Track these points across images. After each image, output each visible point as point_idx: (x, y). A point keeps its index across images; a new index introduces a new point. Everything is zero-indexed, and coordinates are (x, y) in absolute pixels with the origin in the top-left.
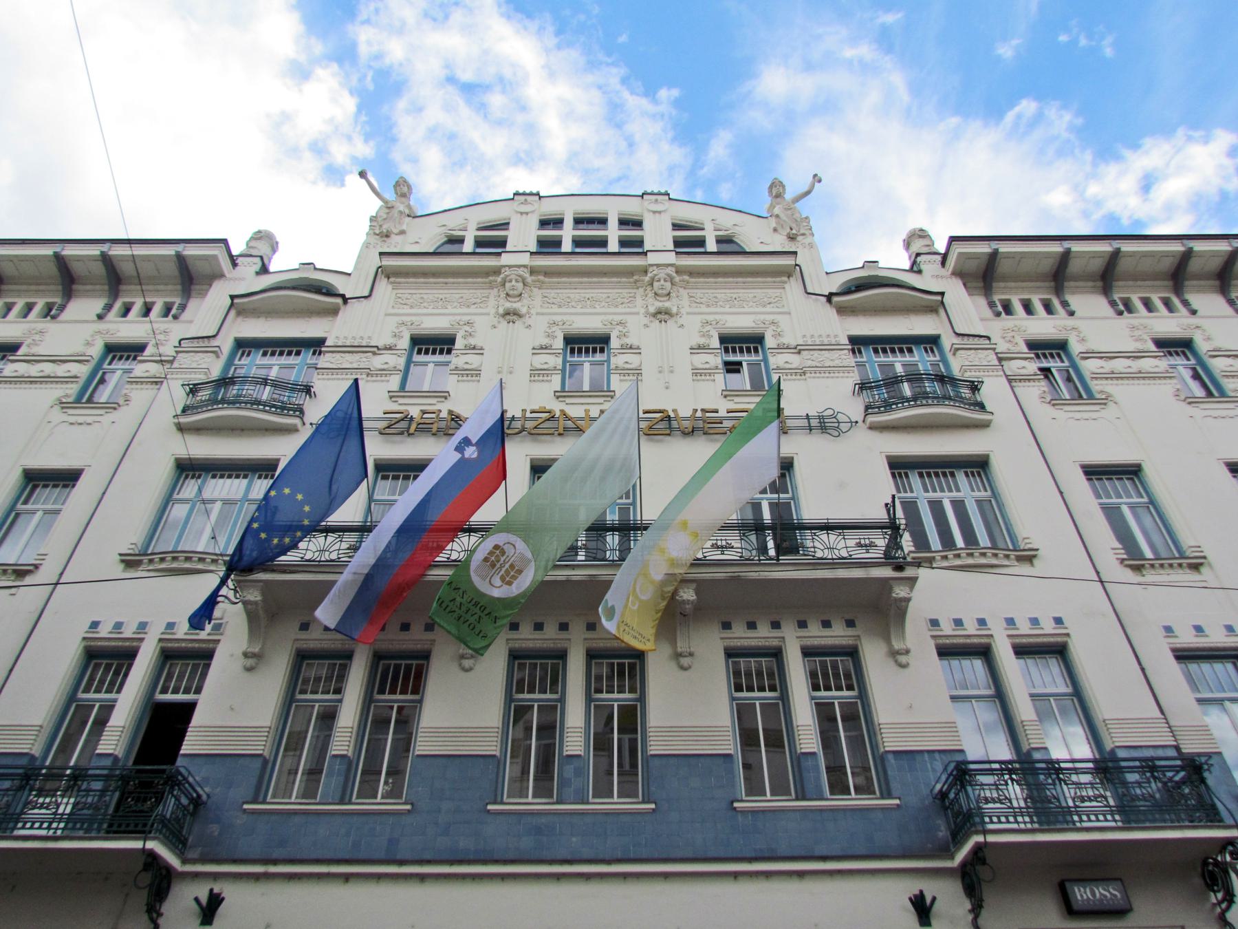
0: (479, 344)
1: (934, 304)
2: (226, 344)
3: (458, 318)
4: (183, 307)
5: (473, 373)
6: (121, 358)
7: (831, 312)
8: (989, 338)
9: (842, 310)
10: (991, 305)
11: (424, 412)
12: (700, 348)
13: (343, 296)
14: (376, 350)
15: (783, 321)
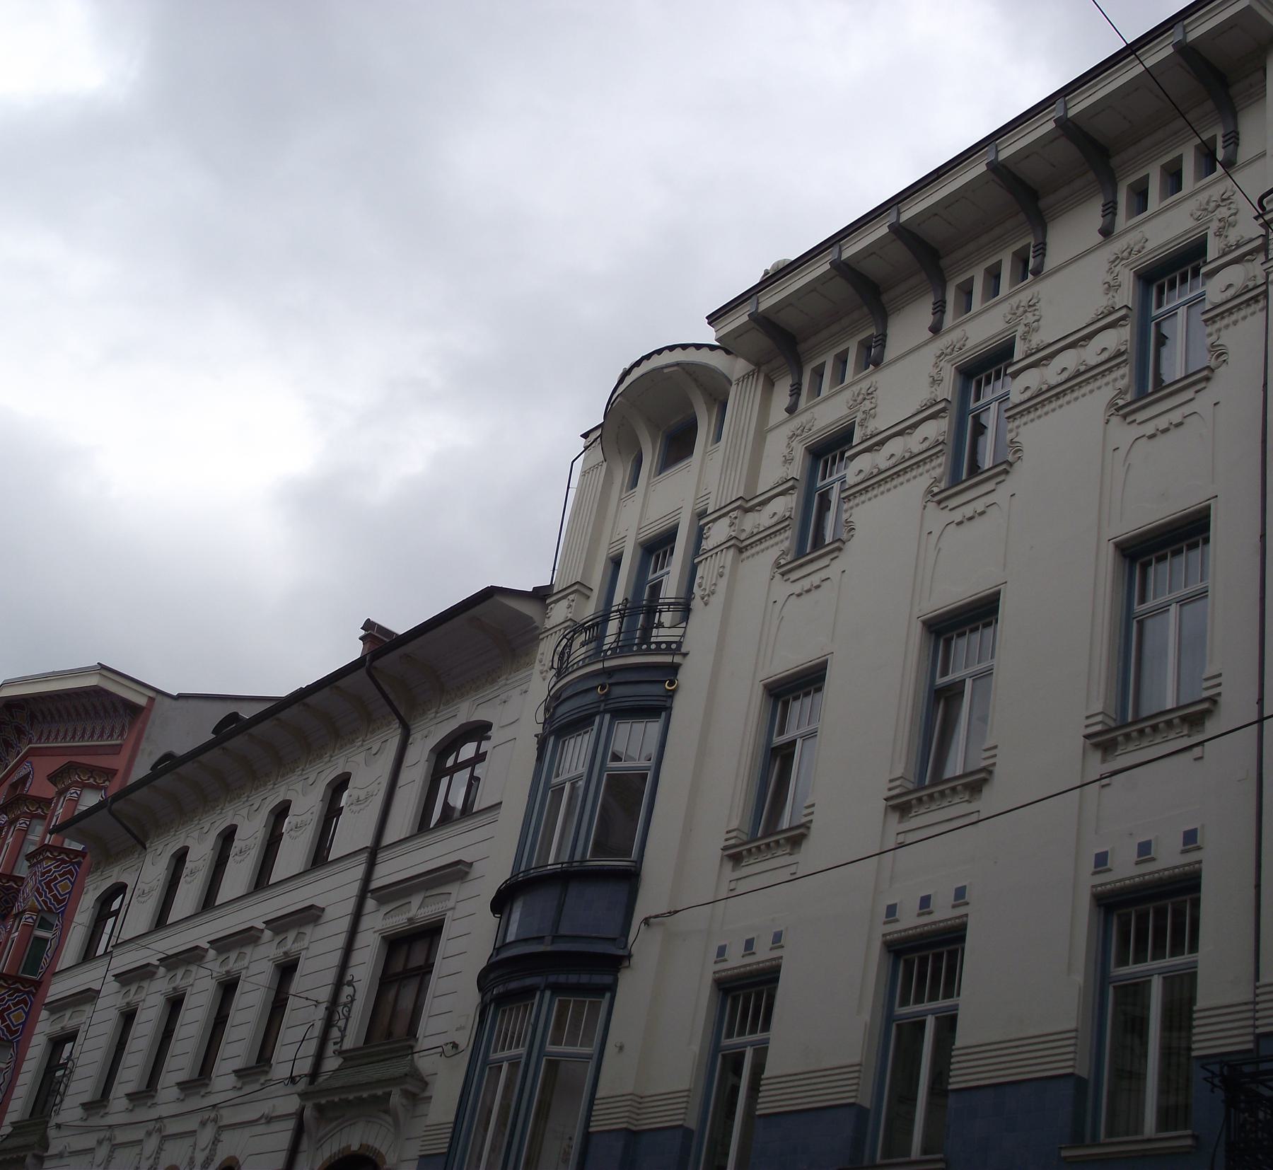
6: (1172, 286)
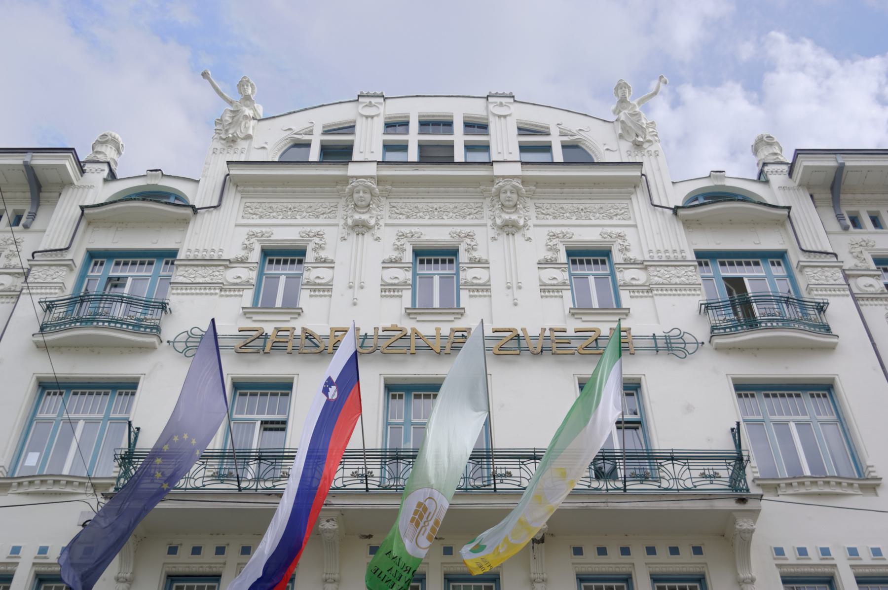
0: (330, 257)
1: (782, 217)
2: (78, 256)
3: (308, 229)
4: (33, 216)
5: (324, 289)
7: (679, 228)
8: (836, 255)
9: (688, 224)
10: (839, 217)
11: (279, 330)
12: (544, 263)
13: (193, 207)
14: (228, 264)
15: (629, 233)
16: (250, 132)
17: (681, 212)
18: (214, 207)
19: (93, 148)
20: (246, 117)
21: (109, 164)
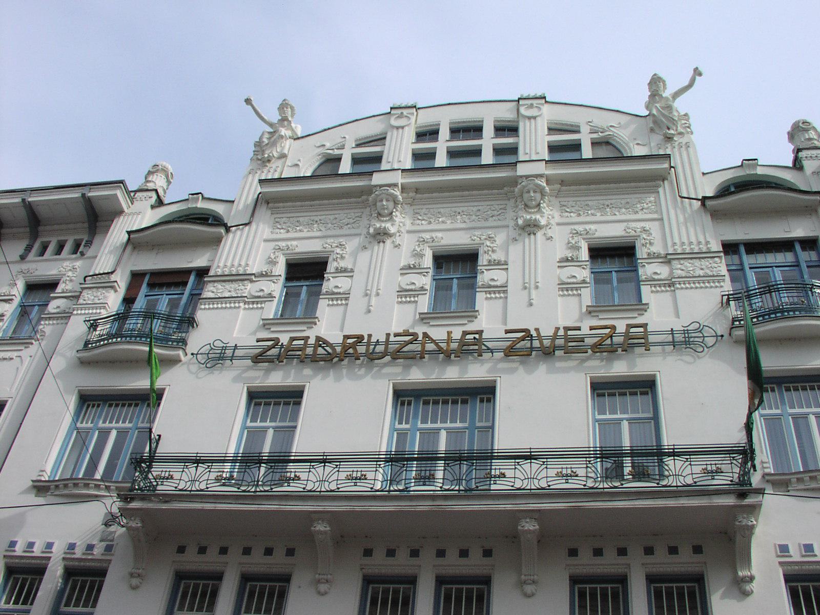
4: (89, 243)
7: (707, 219)
9: (717, 215)
16: (286, 151)
17: (709, 203)
18: (246, 224)
19: (146, 178)
20: (282, 137)
21: (156, 191)
